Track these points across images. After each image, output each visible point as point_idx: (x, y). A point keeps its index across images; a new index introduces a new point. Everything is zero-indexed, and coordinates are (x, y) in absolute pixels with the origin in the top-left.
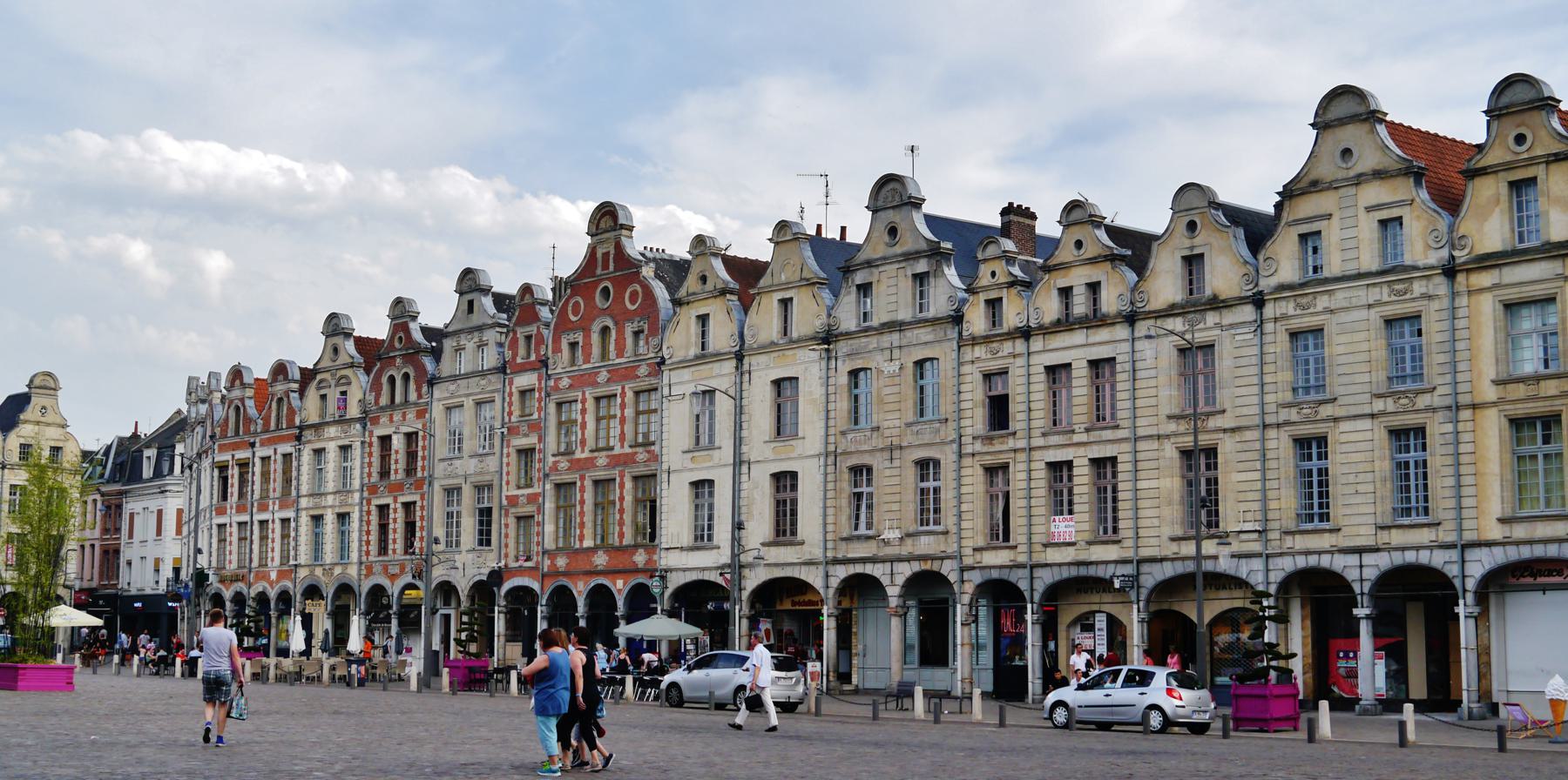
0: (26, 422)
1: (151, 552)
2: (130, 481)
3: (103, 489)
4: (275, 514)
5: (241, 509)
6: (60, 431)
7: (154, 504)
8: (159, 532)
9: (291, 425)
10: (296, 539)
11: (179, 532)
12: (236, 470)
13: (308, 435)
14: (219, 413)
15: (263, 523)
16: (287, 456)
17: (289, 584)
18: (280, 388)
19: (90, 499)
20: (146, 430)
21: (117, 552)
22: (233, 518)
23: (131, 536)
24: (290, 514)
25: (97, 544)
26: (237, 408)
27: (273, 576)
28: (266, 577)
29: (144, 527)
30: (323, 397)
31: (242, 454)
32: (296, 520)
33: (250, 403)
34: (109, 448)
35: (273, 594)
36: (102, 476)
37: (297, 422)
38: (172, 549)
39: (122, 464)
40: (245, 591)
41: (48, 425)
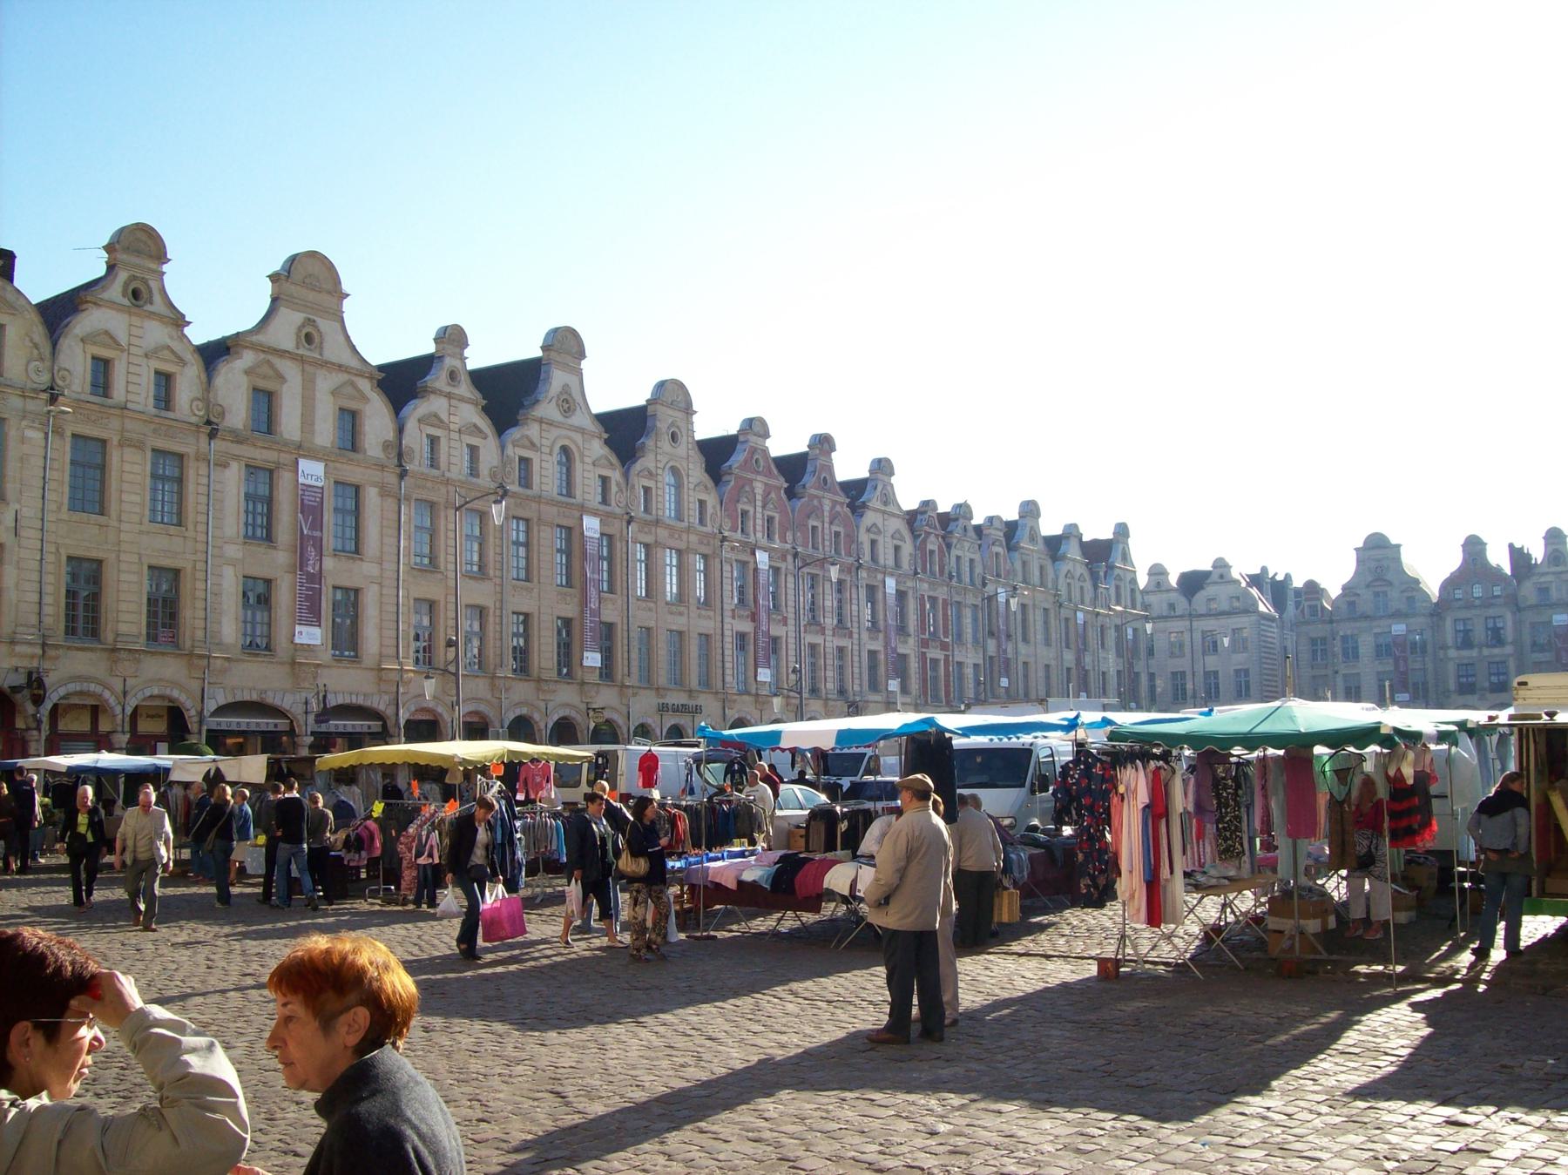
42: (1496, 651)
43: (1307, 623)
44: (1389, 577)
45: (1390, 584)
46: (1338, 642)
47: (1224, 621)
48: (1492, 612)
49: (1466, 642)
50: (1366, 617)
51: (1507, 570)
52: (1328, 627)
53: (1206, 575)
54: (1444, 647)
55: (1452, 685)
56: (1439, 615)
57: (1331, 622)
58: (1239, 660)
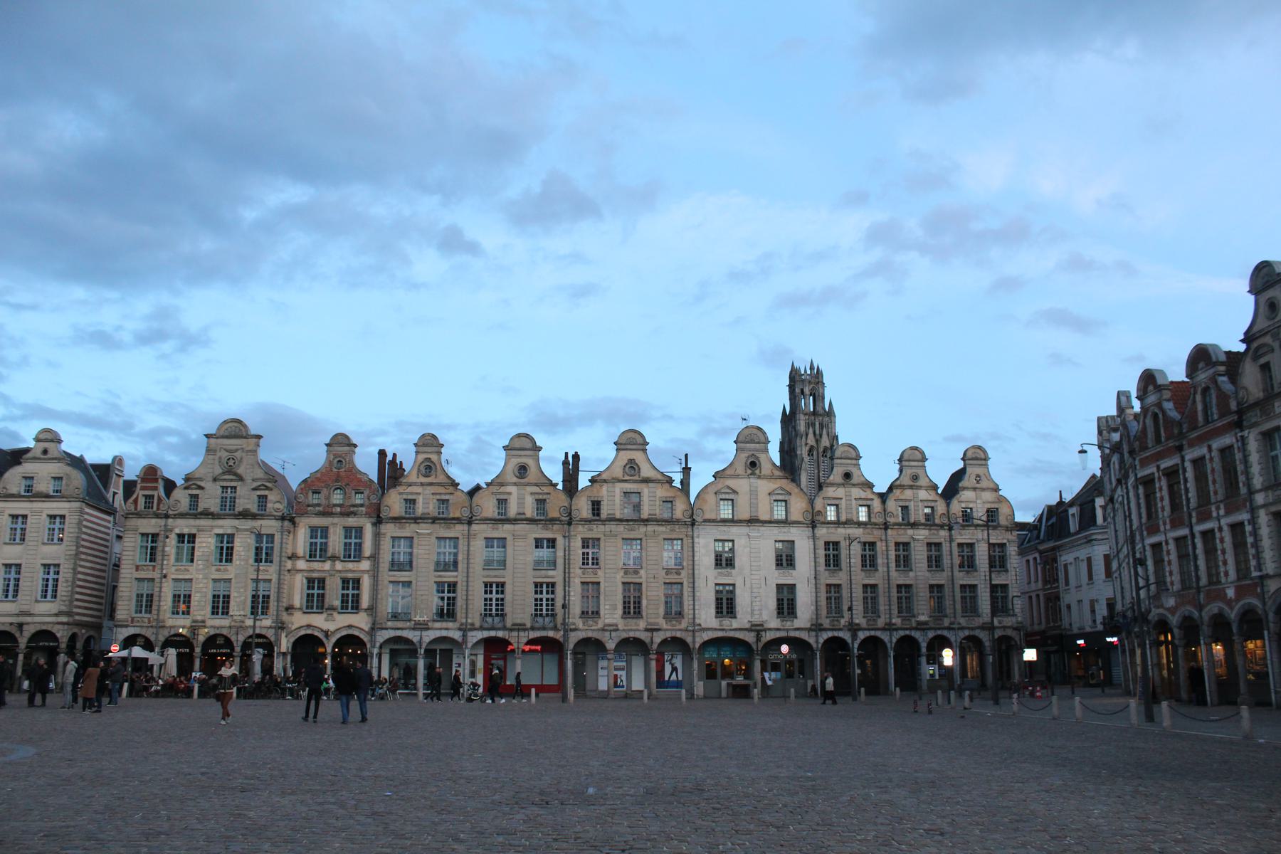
0: (964, 488)
1: (1087, 594)
2: (1060, 537)
3: (1041, 547)
4: (1221, 521)
5: (1175, 524)
6: (994, 494)
7: (1083, 553)
8: (1090, 577)
9: (1224, 412)
10: (1256, 545)
11: (1109, 573)
12: (1164, 483)
13: (1253, 416)
14: (1134, 427)
15: (1208, 535)
16: (1226, 452)
17: (1254, 601)
18: (1203, 376)
19: (1031, 558)
20: (1068, 497)
21: (1058, 598)
22: (1168, 536)
23: (1067, 583)
24: (1244, 516)
25: (1041, 594)
26: (1155, 416)
27: (1231, 593)
28: (1221, 596)
29: (1077, 574)
30: (1266, 368)
31: (1166, 463)
32: (1253, 521)
33: (1168, 406)
34: (1042, 515)
35: (1233, 615)
36: (1038, 537)
37: (1233, 405)
38: (1103, 591)
39: (1052, 525)
40: (1196, 614)
41: (983, 490)
42: (350, 566)
43: (139, 515)
44: (240, 471)
45: (241, 478)
46: (172, 541)
47: (38, 505)
48: (351, 521)
49: (318, 552)
50: (207, 514)
51: (374, 476)
52: (162, 522)
53: (27, 450)
54: (293, 557)
55: (298, 601)
56: (292, 521)
57: (167, 516)
58: (53, 553)
